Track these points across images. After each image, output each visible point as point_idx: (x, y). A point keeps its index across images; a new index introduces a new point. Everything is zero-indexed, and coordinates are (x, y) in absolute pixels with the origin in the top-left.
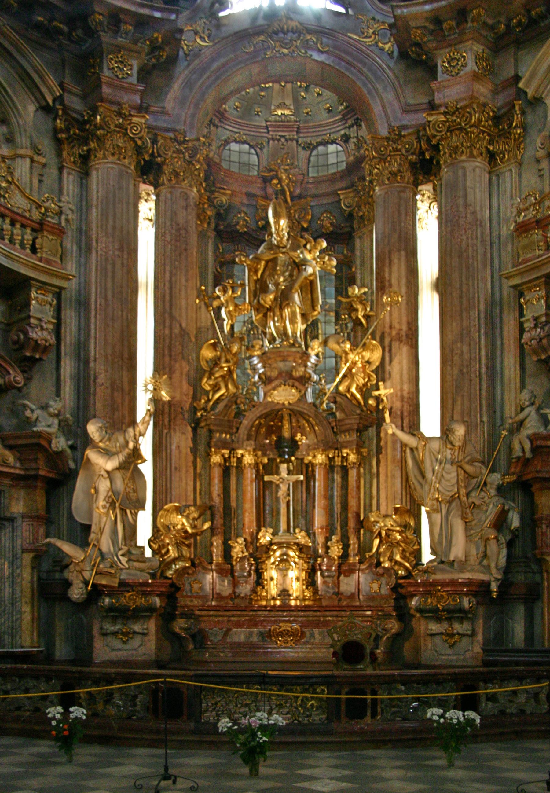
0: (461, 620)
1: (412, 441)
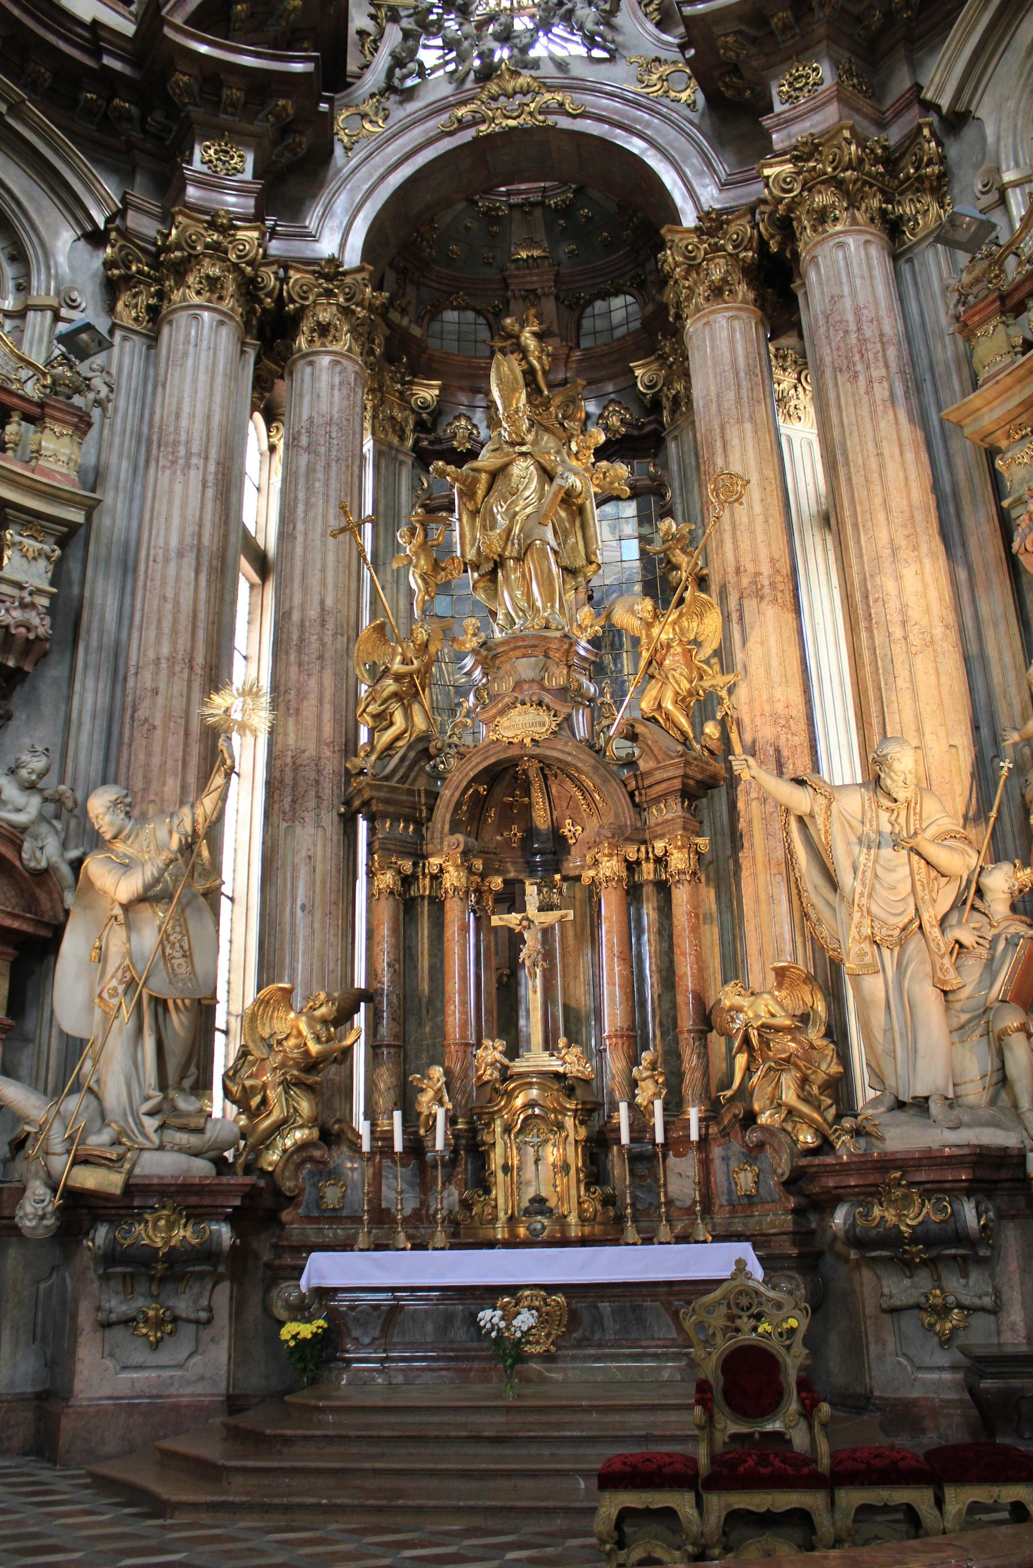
0: (963, 1266)
1: (801, 800)
